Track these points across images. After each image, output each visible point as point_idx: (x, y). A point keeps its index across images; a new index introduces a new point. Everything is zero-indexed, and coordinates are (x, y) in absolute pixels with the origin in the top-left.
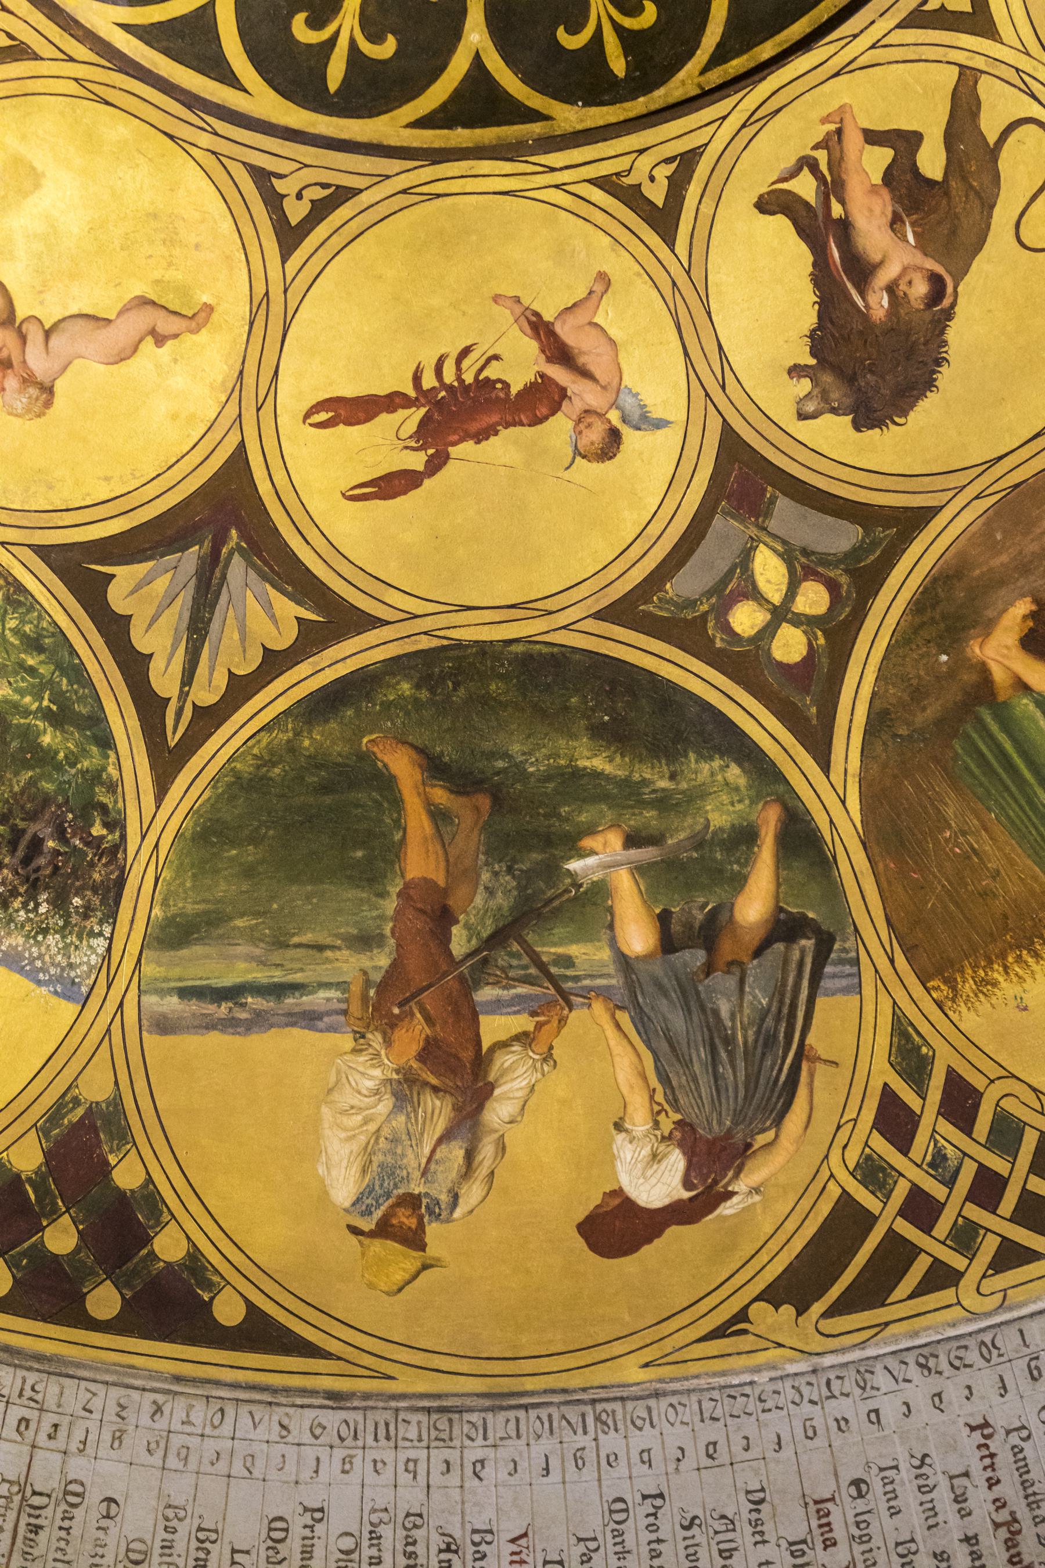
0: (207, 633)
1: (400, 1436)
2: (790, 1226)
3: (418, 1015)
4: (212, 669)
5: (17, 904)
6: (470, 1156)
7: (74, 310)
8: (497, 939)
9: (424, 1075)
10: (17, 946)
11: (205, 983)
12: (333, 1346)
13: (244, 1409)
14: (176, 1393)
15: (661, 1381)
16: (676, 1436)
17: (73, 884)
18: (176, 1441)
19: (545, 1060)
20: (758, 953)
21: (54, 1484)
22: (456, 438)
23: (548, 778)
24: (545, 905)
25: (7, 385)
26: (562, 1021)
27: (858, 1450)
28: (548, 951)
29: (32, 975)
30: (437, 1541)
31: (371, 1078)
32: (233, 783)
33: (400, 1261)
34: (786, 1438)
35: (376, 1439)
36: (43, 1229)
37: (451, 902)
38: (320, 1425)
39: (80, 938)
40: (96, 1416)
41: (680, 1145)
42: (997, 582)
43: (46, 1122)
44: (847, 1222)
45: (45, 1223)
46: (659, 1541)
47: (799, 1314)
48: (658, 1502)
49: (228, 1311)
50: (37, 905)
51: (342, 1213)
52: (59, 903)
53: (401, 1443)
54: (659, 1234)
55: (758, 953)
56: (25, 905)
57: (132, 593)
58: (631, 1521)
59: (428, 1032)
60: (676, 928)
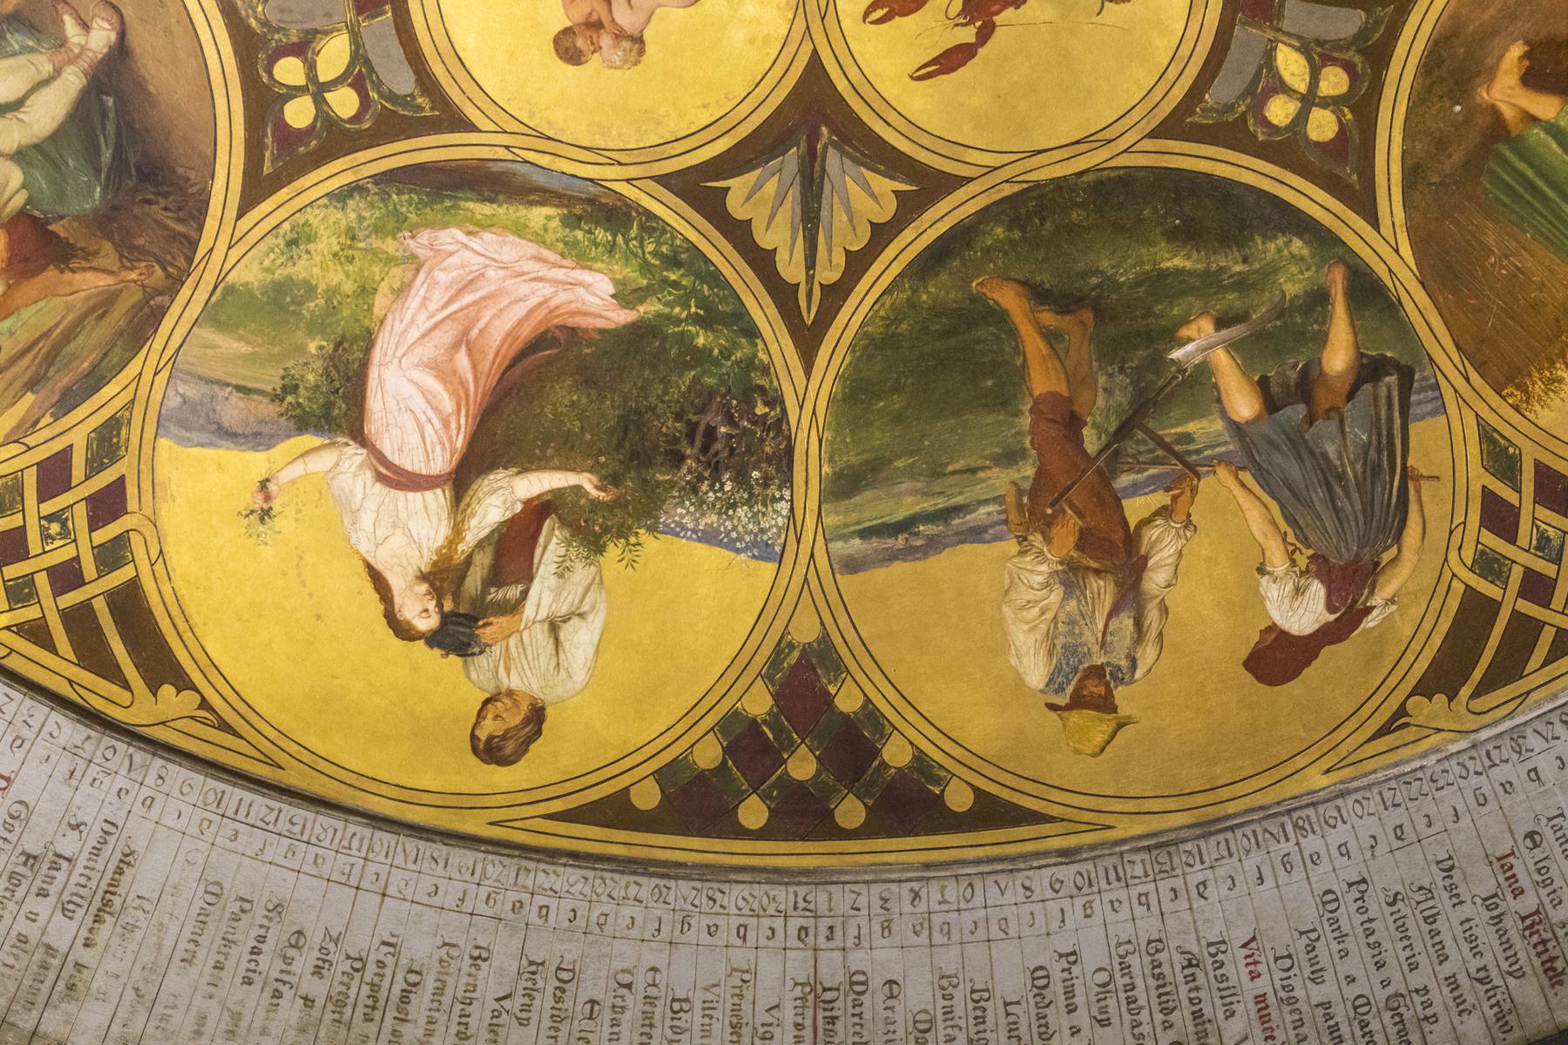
2: (1427, 626)
4: (830, 250)
5: (704, 488)
6: (1138, 623)
8: (1123, 431)
12: (1055, 811)
13: (990, 880)
14: (929, 879)
15: (1343, 782)
16: (1367, 826)
18: (937, 920)
19: (1186, 527)
20: (1350, 396)
21: (840, 978)
22: (996, 8)
23: (1138, 284)
26: (1194, 490)
27: (1524, 809)
28: (1170, 432)
29: (730, 546)
30: (1179, 960)
31: (1040, 573)
33: (1097, 727)
34: (1461, 808)
35: (1109, 883)
36: (785, 761)
37: (1076, 408)
39: (765, 505)
40: (864, 912)
41: (1318, 576)
42: (1489, 33)
44: (1476, 611)
46: (1370, 920)
47: (1450, 700)
48: (1363, 887)
49: (959, 799)
50: (722, 485)
52: (741, 478)
53: (1130, 882)
54: (1316, 657)
55: (1350, 396)
56: (712, 487)
57: (748, 199)
58: (1342, 909)
60: (1275, 389)
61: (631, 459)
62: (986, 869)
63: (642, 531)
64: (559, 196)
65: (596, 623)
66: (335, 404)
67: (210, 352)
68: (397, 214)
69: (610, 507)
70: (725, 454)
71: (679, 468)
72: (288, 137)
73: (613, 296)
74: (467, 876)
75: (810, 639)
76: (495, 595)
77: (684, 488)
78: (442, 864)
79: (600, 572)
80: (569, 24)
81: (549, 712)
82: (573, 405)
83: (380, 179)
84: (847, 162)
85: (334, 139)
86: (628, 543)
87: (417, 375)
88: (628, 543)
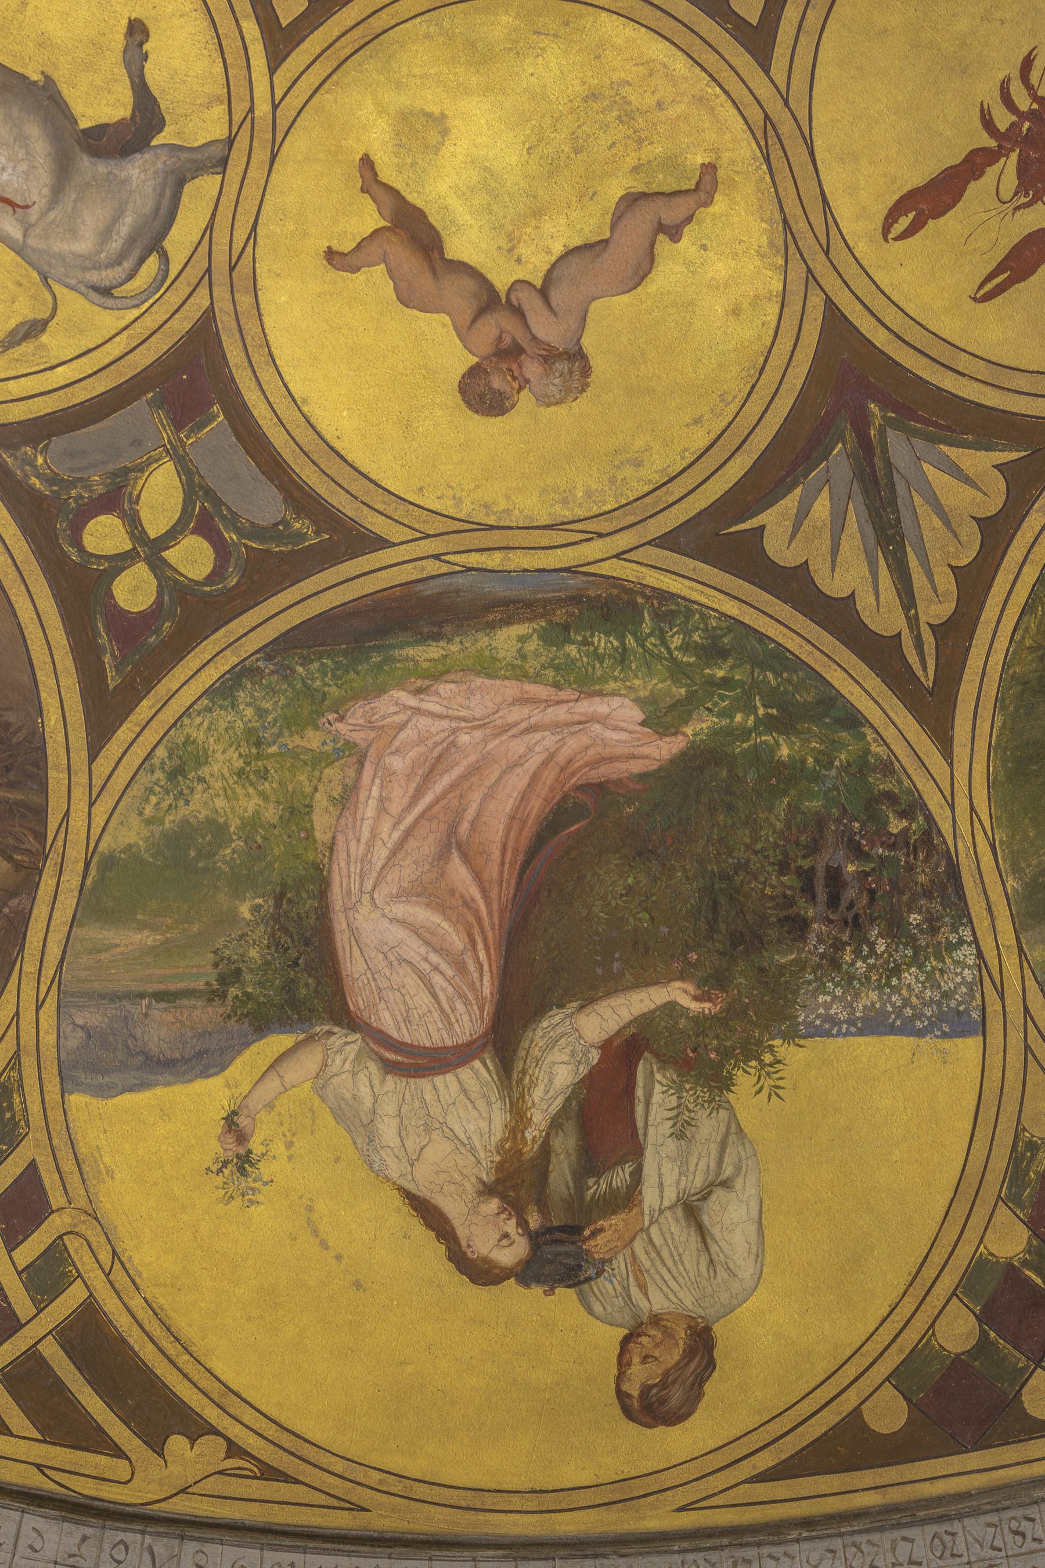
0: (902, 537)
4: (929, 575)
5: (848, 957)
7: (558, 249)
10: (873, 1004)
17: (899, 900)
25: (528, 375)
29: (907, 1029)
32: (1023, 691)
43: (1009, 1188)
50: (872, 946)
52: (896, 929)
56: (857, 953)
57: (793, 536)
61: (734, 945)
63: (777, 1042)
64: (528, 604)
66: (299, 982)
67: (103, 956)
68: (309, 692)
69: (722, 1021)
70: (864, 901)
71: (803, 938)
72: (129, 628)
73: (643, 724)
76: (596, 1187)
77: (819, 966)
79: (733, 1116)
80: (475, 360)
82: (630, 889)
83: (273, 650)
84: (919, 443)
85: (191, 613)
86: (762, 1065)
87: (399, 910)
88: (762, 1065)
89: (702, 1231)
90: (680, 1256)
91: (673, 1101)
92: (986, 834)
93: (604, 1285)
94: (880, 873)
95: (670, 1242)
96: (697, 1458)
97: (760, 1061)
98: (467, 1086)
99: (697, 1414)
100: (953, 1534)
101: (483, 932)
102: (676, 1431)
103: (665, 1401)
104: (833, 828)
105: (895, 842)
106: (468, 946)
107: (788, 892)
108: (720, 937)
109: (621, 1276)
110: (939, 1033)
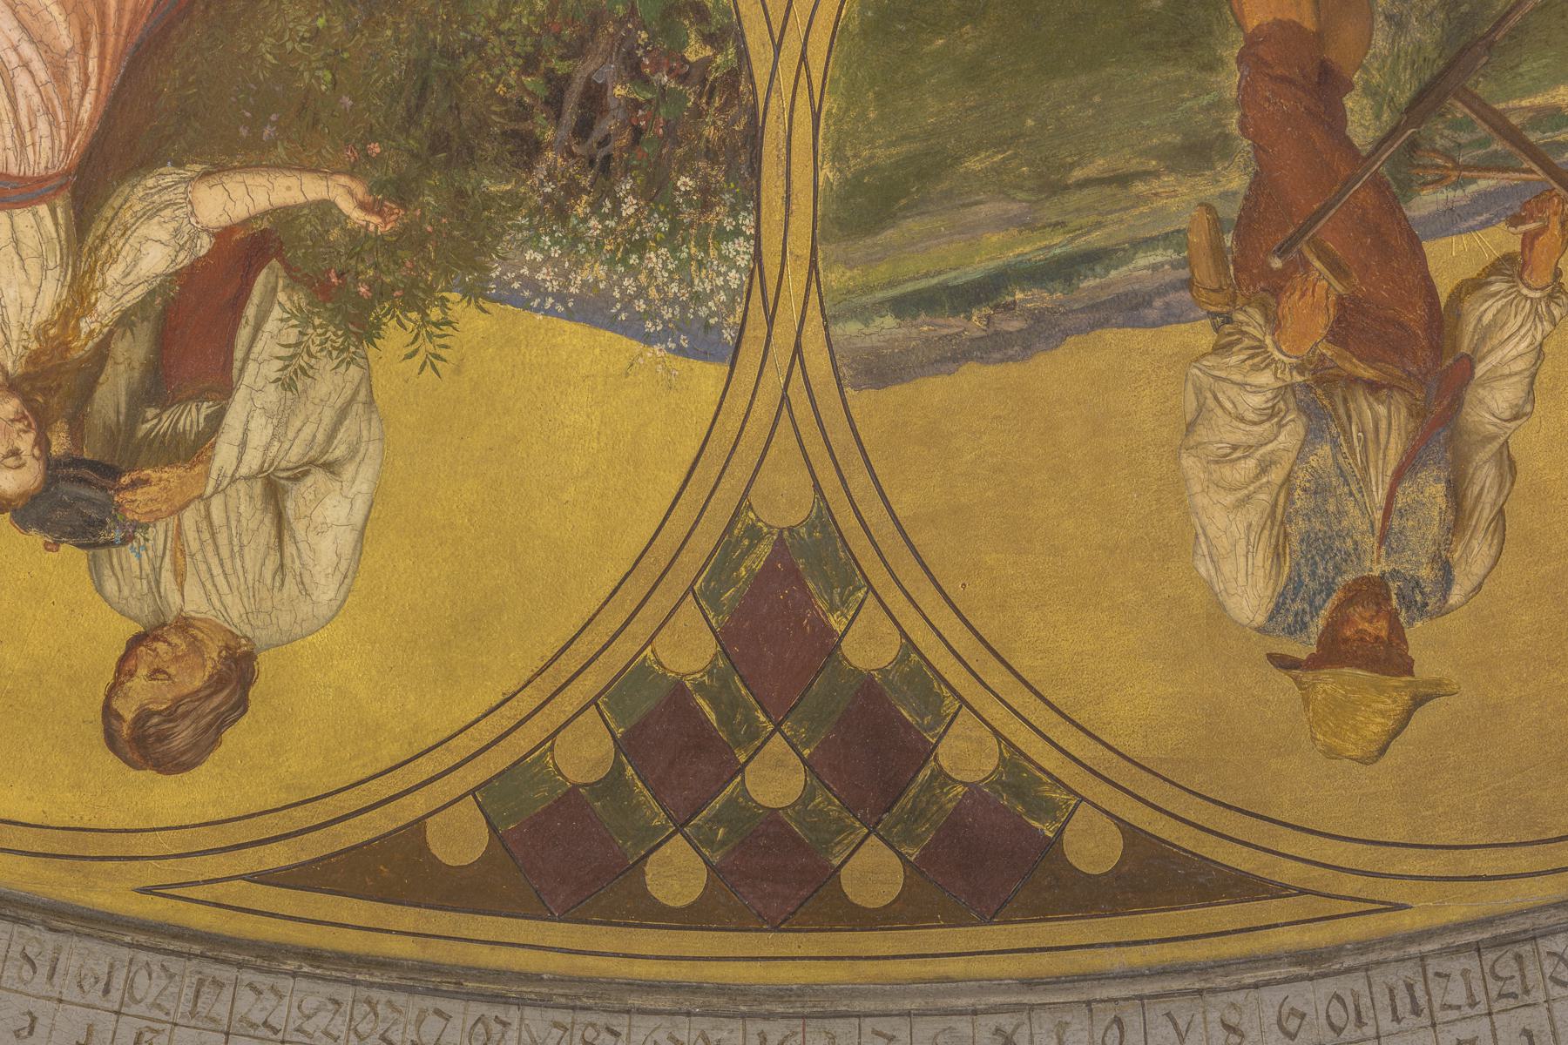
1: (1436, 1005)
3: (1317, 264)
5: (581, 209)
6: (1456, 491)
8: (1426, 101)
9: (1347, 366)
10: (596, 281)
11: (935, 281)
12: (1288, 873)
13: (1156, 1011)
14: (1032, 1007)
17: (671, 153)
19: (1551, 297)
24: (1497, 26)
28: (1519, 105)
29: (632, 329)
31: (1258, 390)
33: (1373, 702)
35: (1397, 1019)
36: (741, 770)
37: (1332, 55)
38: (1293, 1012)
39: (703, 245)
43: (708, 581)
45: (742, 759)
49: (1092, 848)
50: (618, 203)
51: (1256, 636)
52: (655, 190)
53: (1440, 1016)
56: (595, 207)
59: (1340, 289)
61: (434, 150)
62: (1148, 988)
63: (454, 296)
65: (360, 480)
69: (388, 246)
71: (529, 167)
74: (95, 996)
75: (795, 517)
76: (155, 422)
77: (539, 210)
78: (44, 971)
81: (264, 663)
82: (316, 34)
89: (280, 520)
90: (242, 547)
91: (292, 336)
92: (811, 97)
93: (128, 557)
94: (657, 109)
95: (233, 523)
96: (186, 827)
97: (424, 315)
98: (20, 235)
99: (203, 768)
100: (505, 1024)
101: (103, 34)
102: (171, 781)
103: (166, 738)
104: (611, 30)
105: (687, 74)
106: (78, 48)
107: (527, 99)
108: (418, 133)
109: (155, 551)
110: (672, 346)
